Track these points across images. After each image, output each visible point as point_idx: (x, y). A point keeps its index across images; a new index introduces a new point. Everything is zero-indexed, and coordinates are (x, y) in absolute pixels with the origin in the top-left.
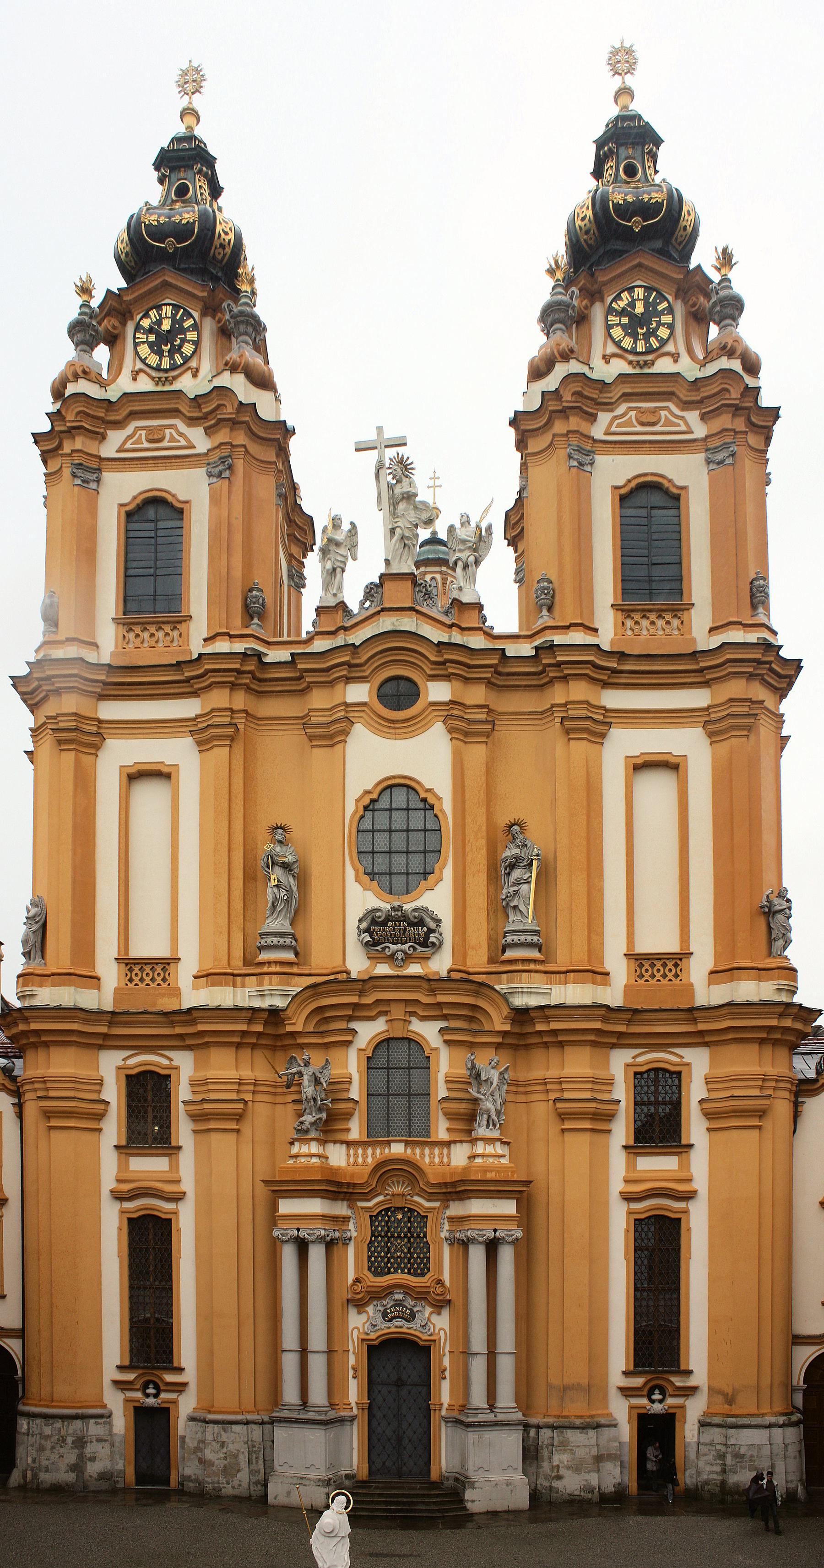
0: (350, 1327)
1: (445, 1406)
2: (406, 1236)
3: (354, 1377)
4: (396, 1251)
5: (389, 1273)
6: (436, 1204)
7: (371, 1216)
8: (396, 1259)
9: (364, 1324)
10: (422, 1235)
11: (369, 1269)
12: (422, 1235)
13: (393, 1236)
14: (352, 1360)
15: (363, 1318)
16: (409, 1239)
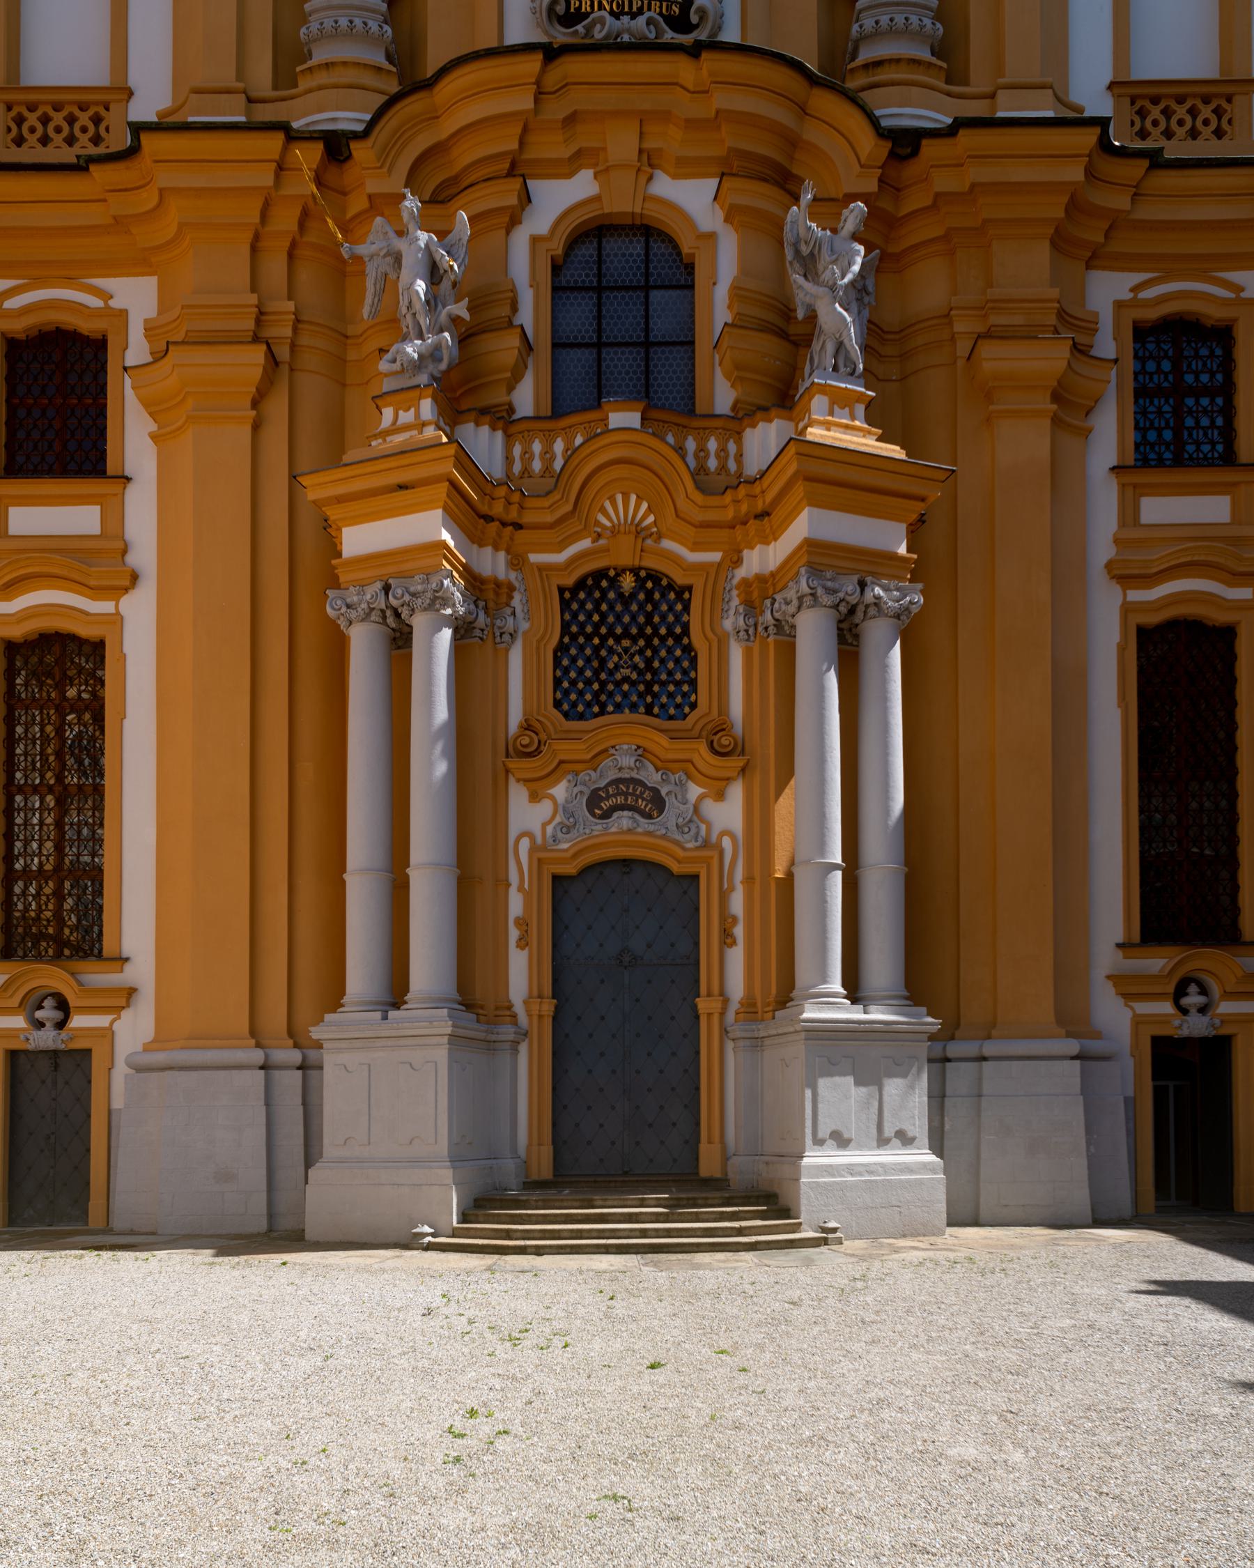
0: (512, 835)
1: (734, 1006)
2: (641, 633)
3: (523, 943)
4: (617, 667)
5: (602, 712)
6: (715, 556)
7: (561, 590)
8: (618, 684)
9: (544, 825)
10: (678, 630)
11: (557, 704)
12: (678, 630)
13: (611, 633)
14: (516, 904)
15: (544, 809)
16: (649, 644)
